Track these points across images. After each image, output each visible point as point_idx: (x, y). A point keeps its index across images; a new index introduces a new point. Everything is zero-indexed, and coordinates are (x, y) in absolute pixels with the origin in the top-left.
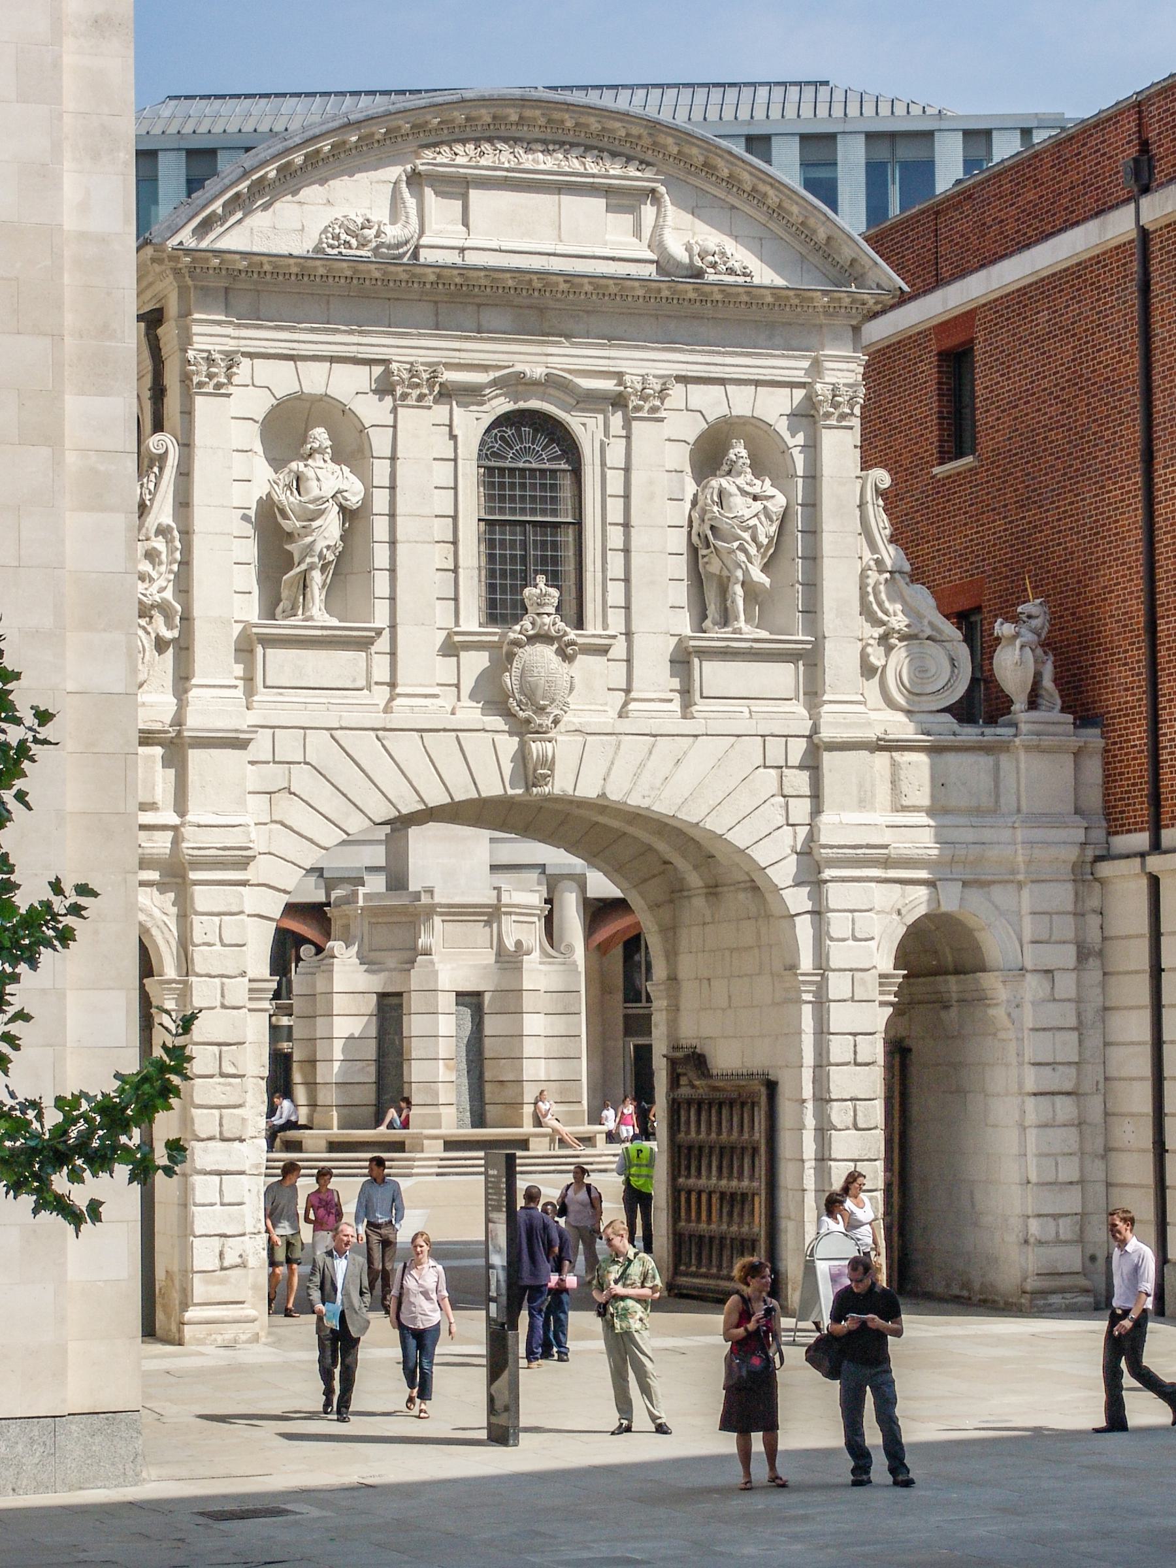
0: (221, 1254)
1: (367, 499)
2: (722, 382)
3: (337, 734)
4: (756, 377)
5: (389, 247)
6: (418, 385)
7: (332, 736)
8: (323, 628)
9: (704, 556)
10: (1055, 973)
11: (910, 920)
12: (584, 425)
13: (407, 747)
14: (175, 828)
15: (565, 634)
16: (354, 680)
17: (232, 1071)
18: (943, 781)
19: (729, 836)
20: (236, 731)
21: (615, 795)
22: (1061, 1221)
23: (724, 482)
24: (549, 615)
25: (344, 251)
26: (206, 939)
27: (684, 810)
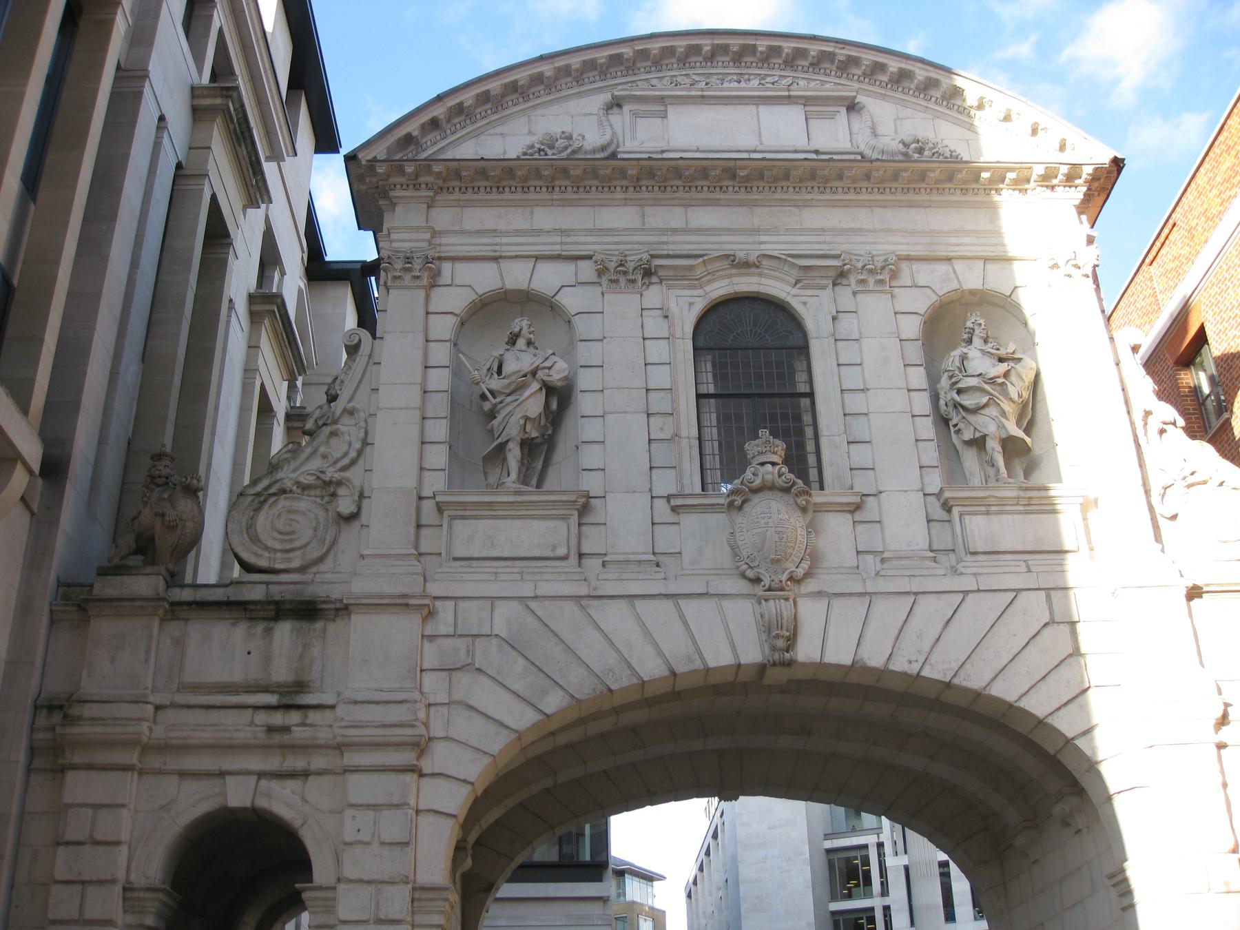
2: (948, 259)
3: (533, 605)
4: (984, 254)
5: (586, 153)
6: (625, 273)
7: (527, 606)
9: (955, 426)
12: (805, 304)
13: (615, 618)
14: (333, 707)
16: (554, 548)
19: (1022, 704)
20: (405, 596)
21: (875, 658)
24: (773, 464)
26: (360, 837)
27: (962, 674)
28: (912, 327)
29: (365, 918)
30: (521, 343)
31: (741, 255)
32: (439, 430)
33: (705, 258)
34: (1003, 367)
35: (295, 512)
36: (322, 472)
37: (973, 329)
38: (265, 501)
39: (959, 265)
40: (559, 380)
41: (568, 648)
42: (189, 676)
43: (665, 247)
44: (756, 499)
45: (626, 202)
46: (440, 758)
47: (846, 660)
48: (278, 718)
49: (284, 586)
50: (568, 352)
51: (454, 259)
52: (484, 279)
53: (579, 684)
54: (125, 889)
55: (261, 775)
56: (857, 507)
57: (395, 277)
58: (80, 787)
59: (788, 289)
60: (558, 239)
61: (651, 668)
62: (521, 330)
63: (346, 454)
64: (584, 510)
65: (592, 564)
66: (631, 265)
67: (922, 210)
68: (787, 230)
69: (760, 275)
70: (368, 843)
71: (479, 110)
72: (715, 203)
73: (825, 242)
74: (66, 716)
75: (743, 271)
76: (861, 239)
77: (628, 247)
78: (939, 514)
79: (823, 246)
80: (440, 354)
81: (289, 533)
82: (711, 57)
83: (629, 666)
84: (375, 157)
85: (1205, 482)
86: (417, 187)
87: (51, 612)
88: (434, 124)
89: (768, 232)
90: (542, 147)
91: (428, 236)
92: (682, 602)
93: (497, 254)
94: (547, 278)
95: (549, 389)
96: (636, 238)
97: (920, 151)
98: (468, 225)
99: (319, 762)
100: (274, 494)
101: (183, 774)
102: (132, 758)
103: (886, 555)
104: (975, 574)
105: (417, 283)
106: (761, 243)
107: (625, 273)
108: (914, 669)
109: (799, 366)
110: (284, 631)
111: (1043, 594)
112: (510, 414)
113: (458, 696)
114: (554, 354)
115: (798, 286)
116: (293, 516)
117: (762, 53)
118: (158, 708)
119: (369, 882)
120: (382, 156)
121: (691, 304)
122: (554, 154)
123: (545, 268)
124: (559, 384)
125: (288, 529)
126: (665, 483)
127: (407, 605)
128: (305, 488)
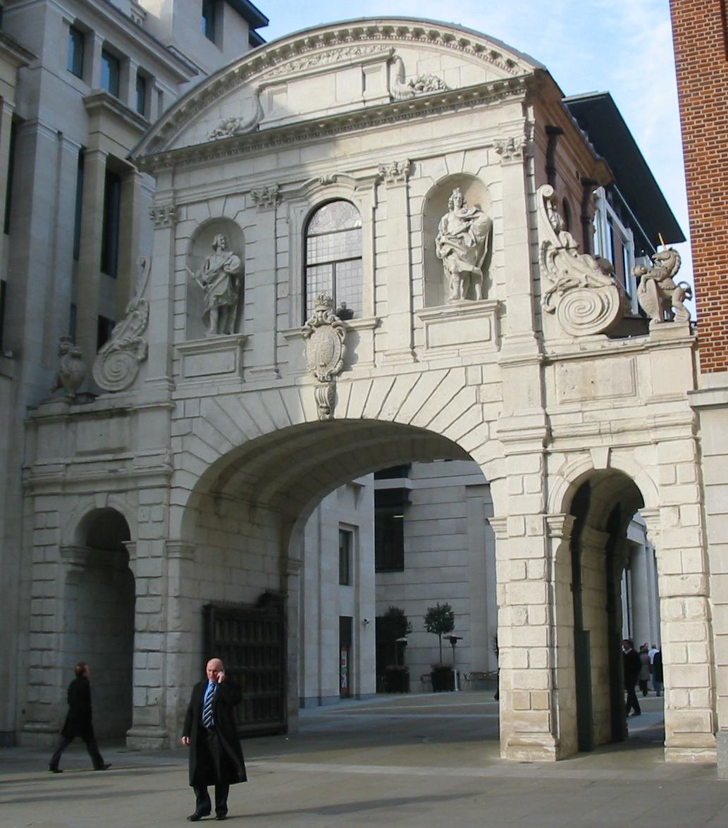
0: (147, 697)
1: (242, 268)
2: (443, 155)
3: (217, 398)
5: (243, 129)
6: (268, 199)
8: (210, 340)
10: (681, 507)
11: (572, 478)
13: (252, 401)
15: (334, 320)
16: (228, 367)
17: (155, 593)
18: (591, 380)
20: (158, 402)
21: (370, 414)
22: (692, 693)
23: (446, 216)
24: (323, 311)
25: (219, 138)
28: (417, 206)
29: (147, 555)
30: (219, 249)
32: (181, 307)
33: (306, 183)
34: (465, 225)
35: (119, 361)
36: (130, 338)
37: (453, 202)
38: (108, 356)
40: (234, 270)
41: (233, 421)
42: (81, 449)
43: (288, 178)
44: (317, 330)
45: (269, 153)
46: (179, 479)
47: (358, 417)
48: (114, 466)
49: (117, 402)
50: (240, 254)
51: (187, 205)
53: (237, 439)
54: (61, 548)
55: (110, 492)
57: (157, 224)
58: (42, 504)
59: (352, 192)
60: (235, 183)
61: (268, 428)
62: (217, 243)
63: (140, 327)
66: (270, 194)
67: (429, 124)
68: (351, 155)
69: (337, 186)
70: (147, 522)
71: (193, 109)
72: (315, 143)
73: (372, 159)
74: (32, 473)
75: (329, 185)
76: (392, 152)
77: (269, 181)
79: (372, 161)
80: (181, 263)
81: (118, 372)
82: (313, 43)
83: (258, 427)
84: (140, 155)
85: (577, 286)
86: (165, 166)
87: (25, 424)
88: (169, 125)
89: (340, 158)
90: (220, 130)
91: (171, 194)
92: (281, 391)
93: (206, 198)
95: (233, 277)
96: (274, 175)
97: (422, 88)
98: (193, 183)
99: (131, 485)
100: (111, 352)
101: (81, 494)
102: (58, 490)
103: (386, 353)
104: (428, 361)
105: (167, 225)
106: (337, 166)
107: (268, 199)
108: (390, 419)
110: (114, 422)
111: (464, 369)
112: (210, 295)
113: (185, 449)
114: (233, 254)
115: (357, 189)
116: (119, 363)
117: (337, 36)
118: (68, 465)
119: (148, 540)
120: (143, 155)
121: (302, 211)
122: (227, 134)
123: (231, 201)
124: (234, 273)
125: (117, 370)
127: (160, 407)
128: (123, 347)
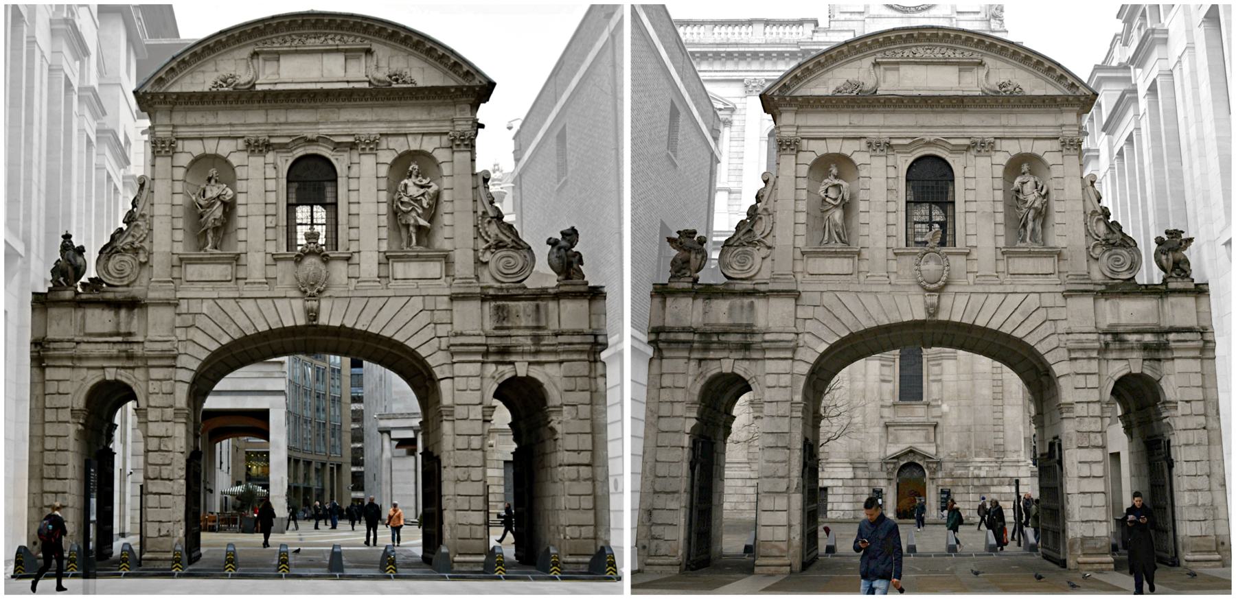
3: (838, 294)
13: (869, 301)
28: (999, 171)
31: (927, 139)
32: (802, 218)
39: (1023, 142)
52: (820, 148)
56: (968, 254)
64: (859, 254)
65: (862, 277)
78: (1000, 257)
94: (847, 148)
109: (951, 188)
123: (847, 143)
126: (893, 244)
